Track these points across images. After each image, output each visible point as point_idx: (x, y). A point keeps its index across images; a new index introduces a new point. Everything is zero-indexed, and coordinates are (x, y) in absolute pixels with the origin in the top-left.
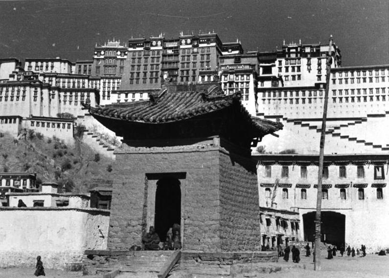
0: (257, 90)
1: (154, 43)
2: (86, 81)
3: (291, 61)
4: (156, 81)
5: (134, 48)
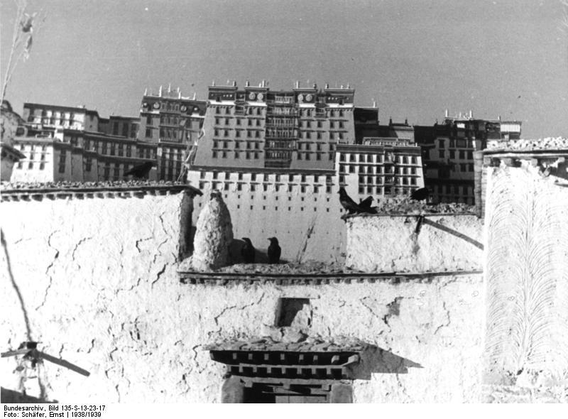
1: (252, 95)
2: (134, 148)
4: (256, 157)
5: (218, 100)
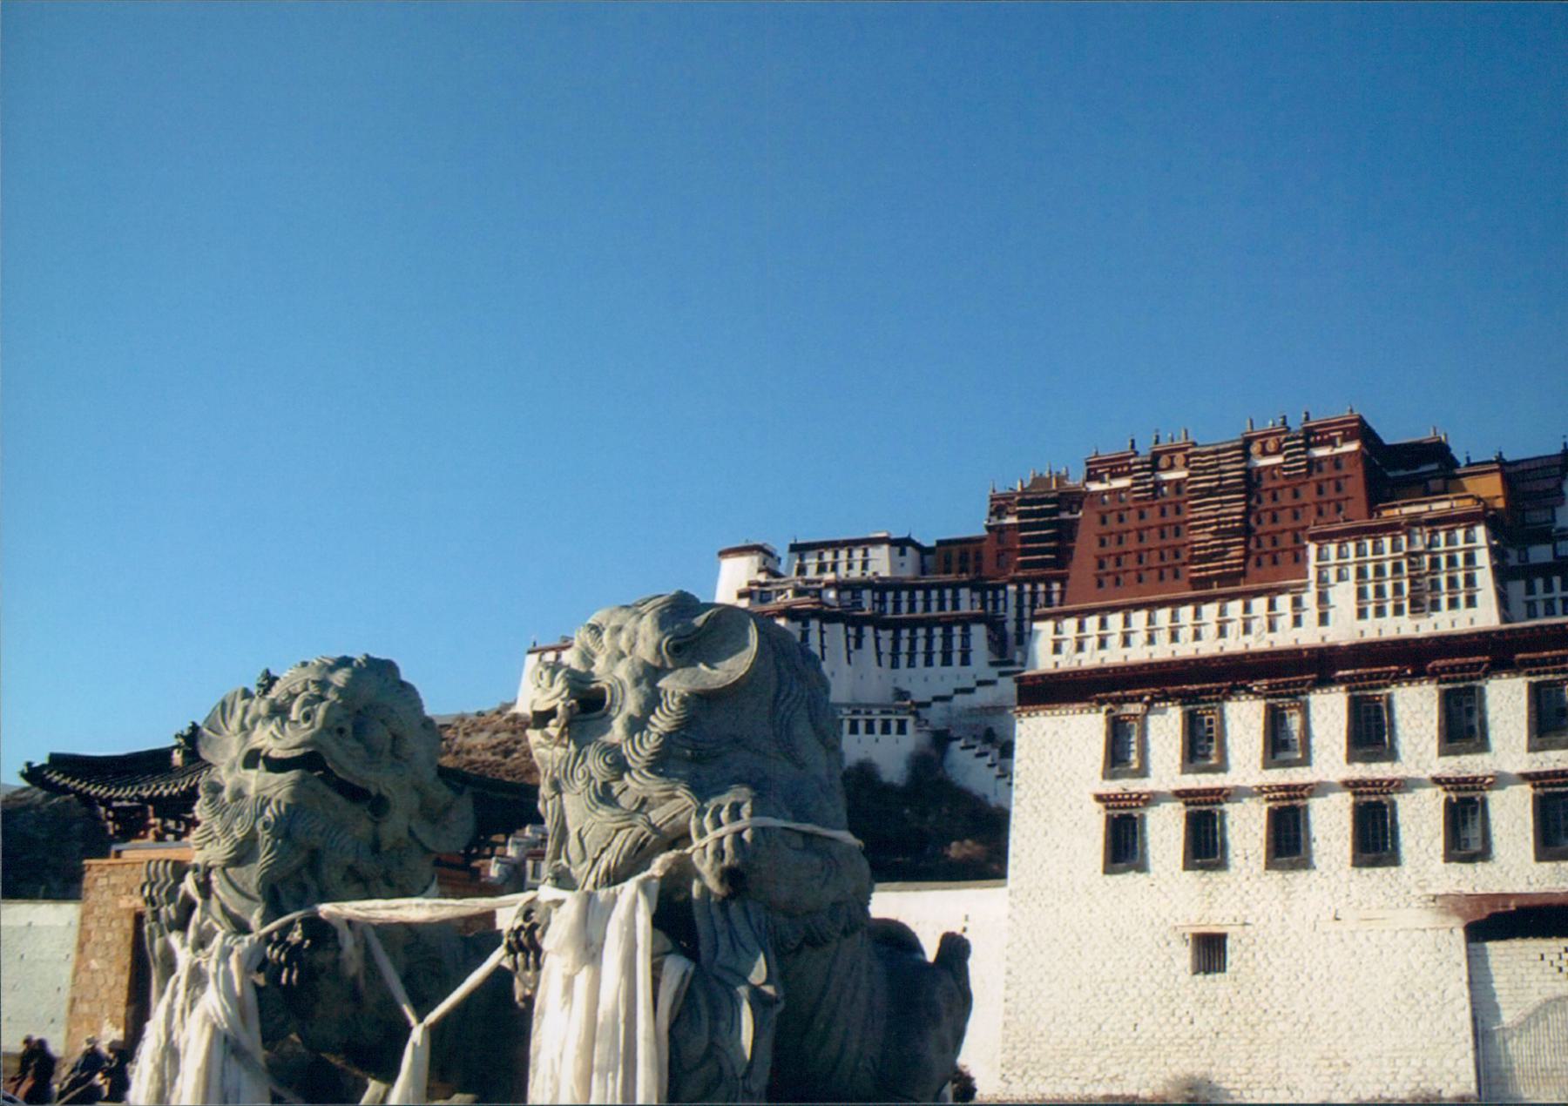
0: (1502, 575)
1: (1164, 461)
2: (964, 593)
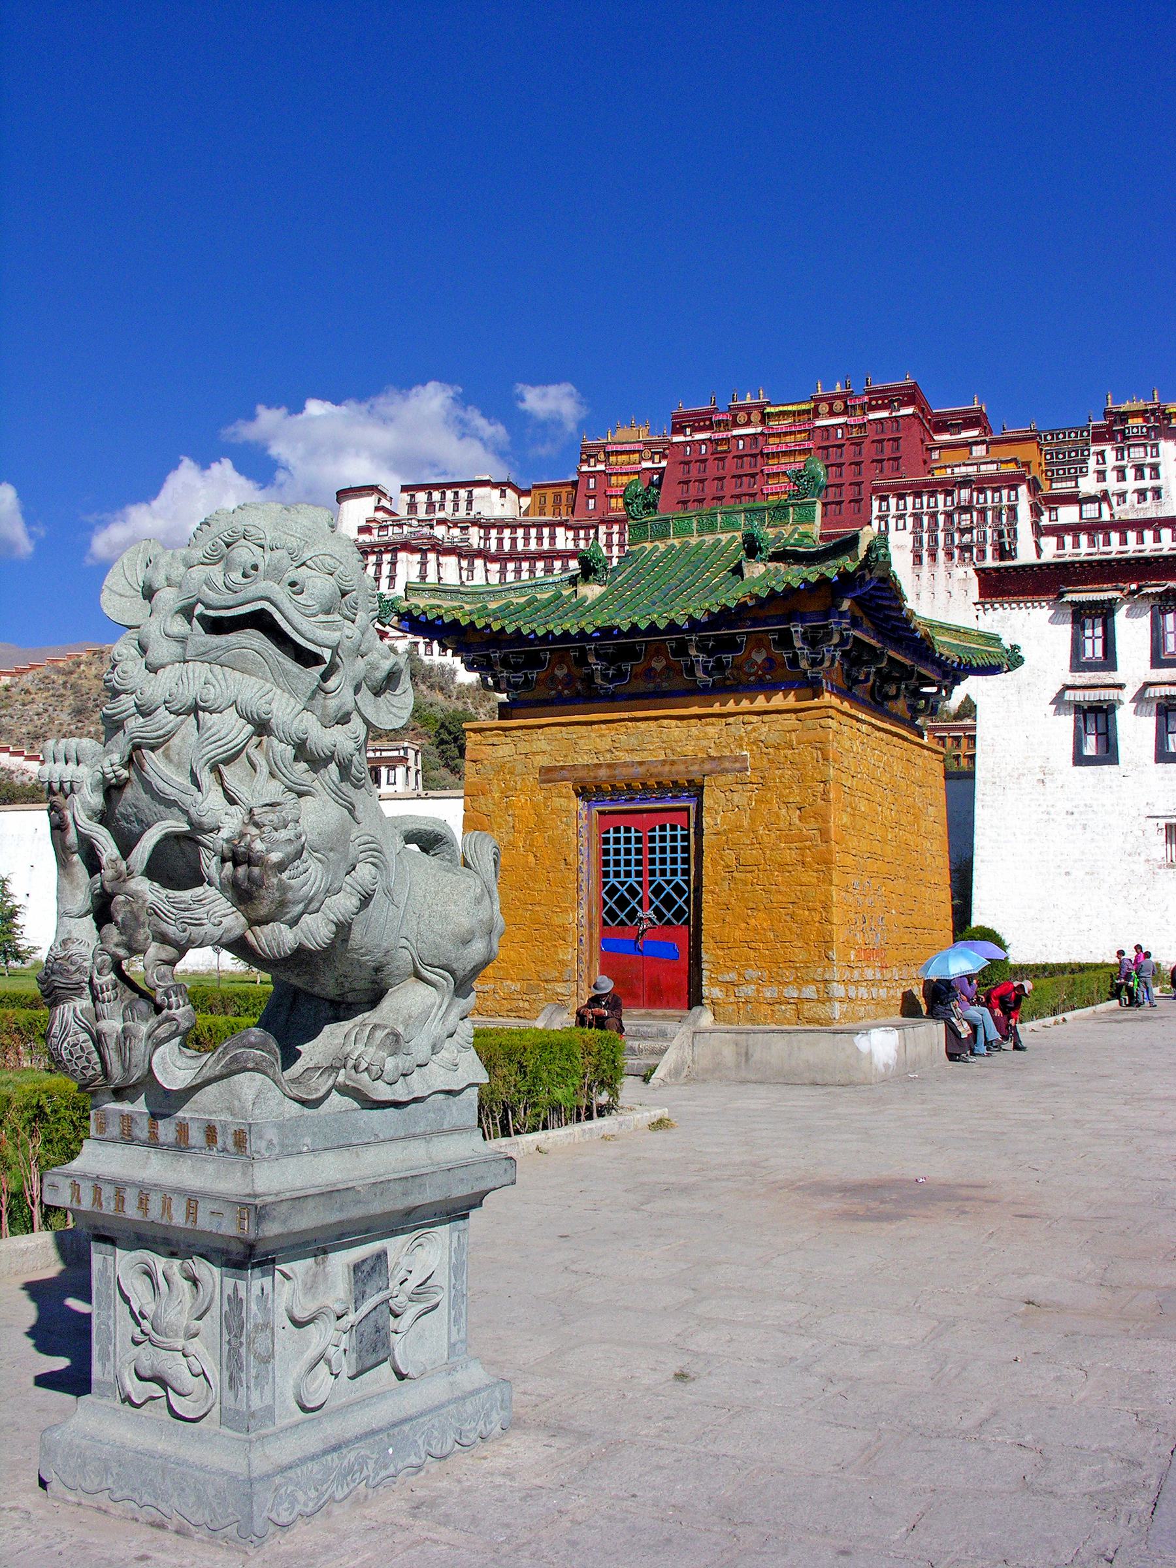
1: (742, 417)
2: (560, 531)
3: (1132, 450)
